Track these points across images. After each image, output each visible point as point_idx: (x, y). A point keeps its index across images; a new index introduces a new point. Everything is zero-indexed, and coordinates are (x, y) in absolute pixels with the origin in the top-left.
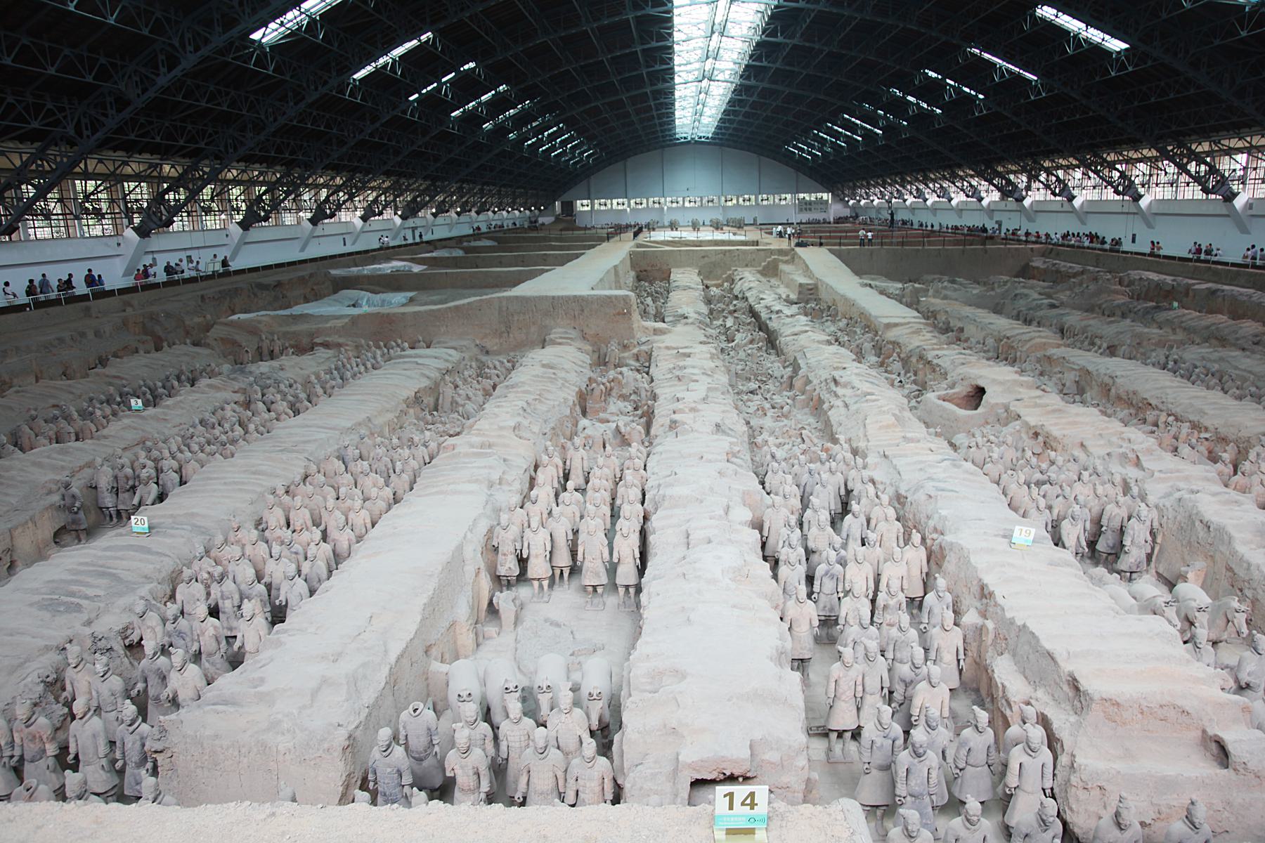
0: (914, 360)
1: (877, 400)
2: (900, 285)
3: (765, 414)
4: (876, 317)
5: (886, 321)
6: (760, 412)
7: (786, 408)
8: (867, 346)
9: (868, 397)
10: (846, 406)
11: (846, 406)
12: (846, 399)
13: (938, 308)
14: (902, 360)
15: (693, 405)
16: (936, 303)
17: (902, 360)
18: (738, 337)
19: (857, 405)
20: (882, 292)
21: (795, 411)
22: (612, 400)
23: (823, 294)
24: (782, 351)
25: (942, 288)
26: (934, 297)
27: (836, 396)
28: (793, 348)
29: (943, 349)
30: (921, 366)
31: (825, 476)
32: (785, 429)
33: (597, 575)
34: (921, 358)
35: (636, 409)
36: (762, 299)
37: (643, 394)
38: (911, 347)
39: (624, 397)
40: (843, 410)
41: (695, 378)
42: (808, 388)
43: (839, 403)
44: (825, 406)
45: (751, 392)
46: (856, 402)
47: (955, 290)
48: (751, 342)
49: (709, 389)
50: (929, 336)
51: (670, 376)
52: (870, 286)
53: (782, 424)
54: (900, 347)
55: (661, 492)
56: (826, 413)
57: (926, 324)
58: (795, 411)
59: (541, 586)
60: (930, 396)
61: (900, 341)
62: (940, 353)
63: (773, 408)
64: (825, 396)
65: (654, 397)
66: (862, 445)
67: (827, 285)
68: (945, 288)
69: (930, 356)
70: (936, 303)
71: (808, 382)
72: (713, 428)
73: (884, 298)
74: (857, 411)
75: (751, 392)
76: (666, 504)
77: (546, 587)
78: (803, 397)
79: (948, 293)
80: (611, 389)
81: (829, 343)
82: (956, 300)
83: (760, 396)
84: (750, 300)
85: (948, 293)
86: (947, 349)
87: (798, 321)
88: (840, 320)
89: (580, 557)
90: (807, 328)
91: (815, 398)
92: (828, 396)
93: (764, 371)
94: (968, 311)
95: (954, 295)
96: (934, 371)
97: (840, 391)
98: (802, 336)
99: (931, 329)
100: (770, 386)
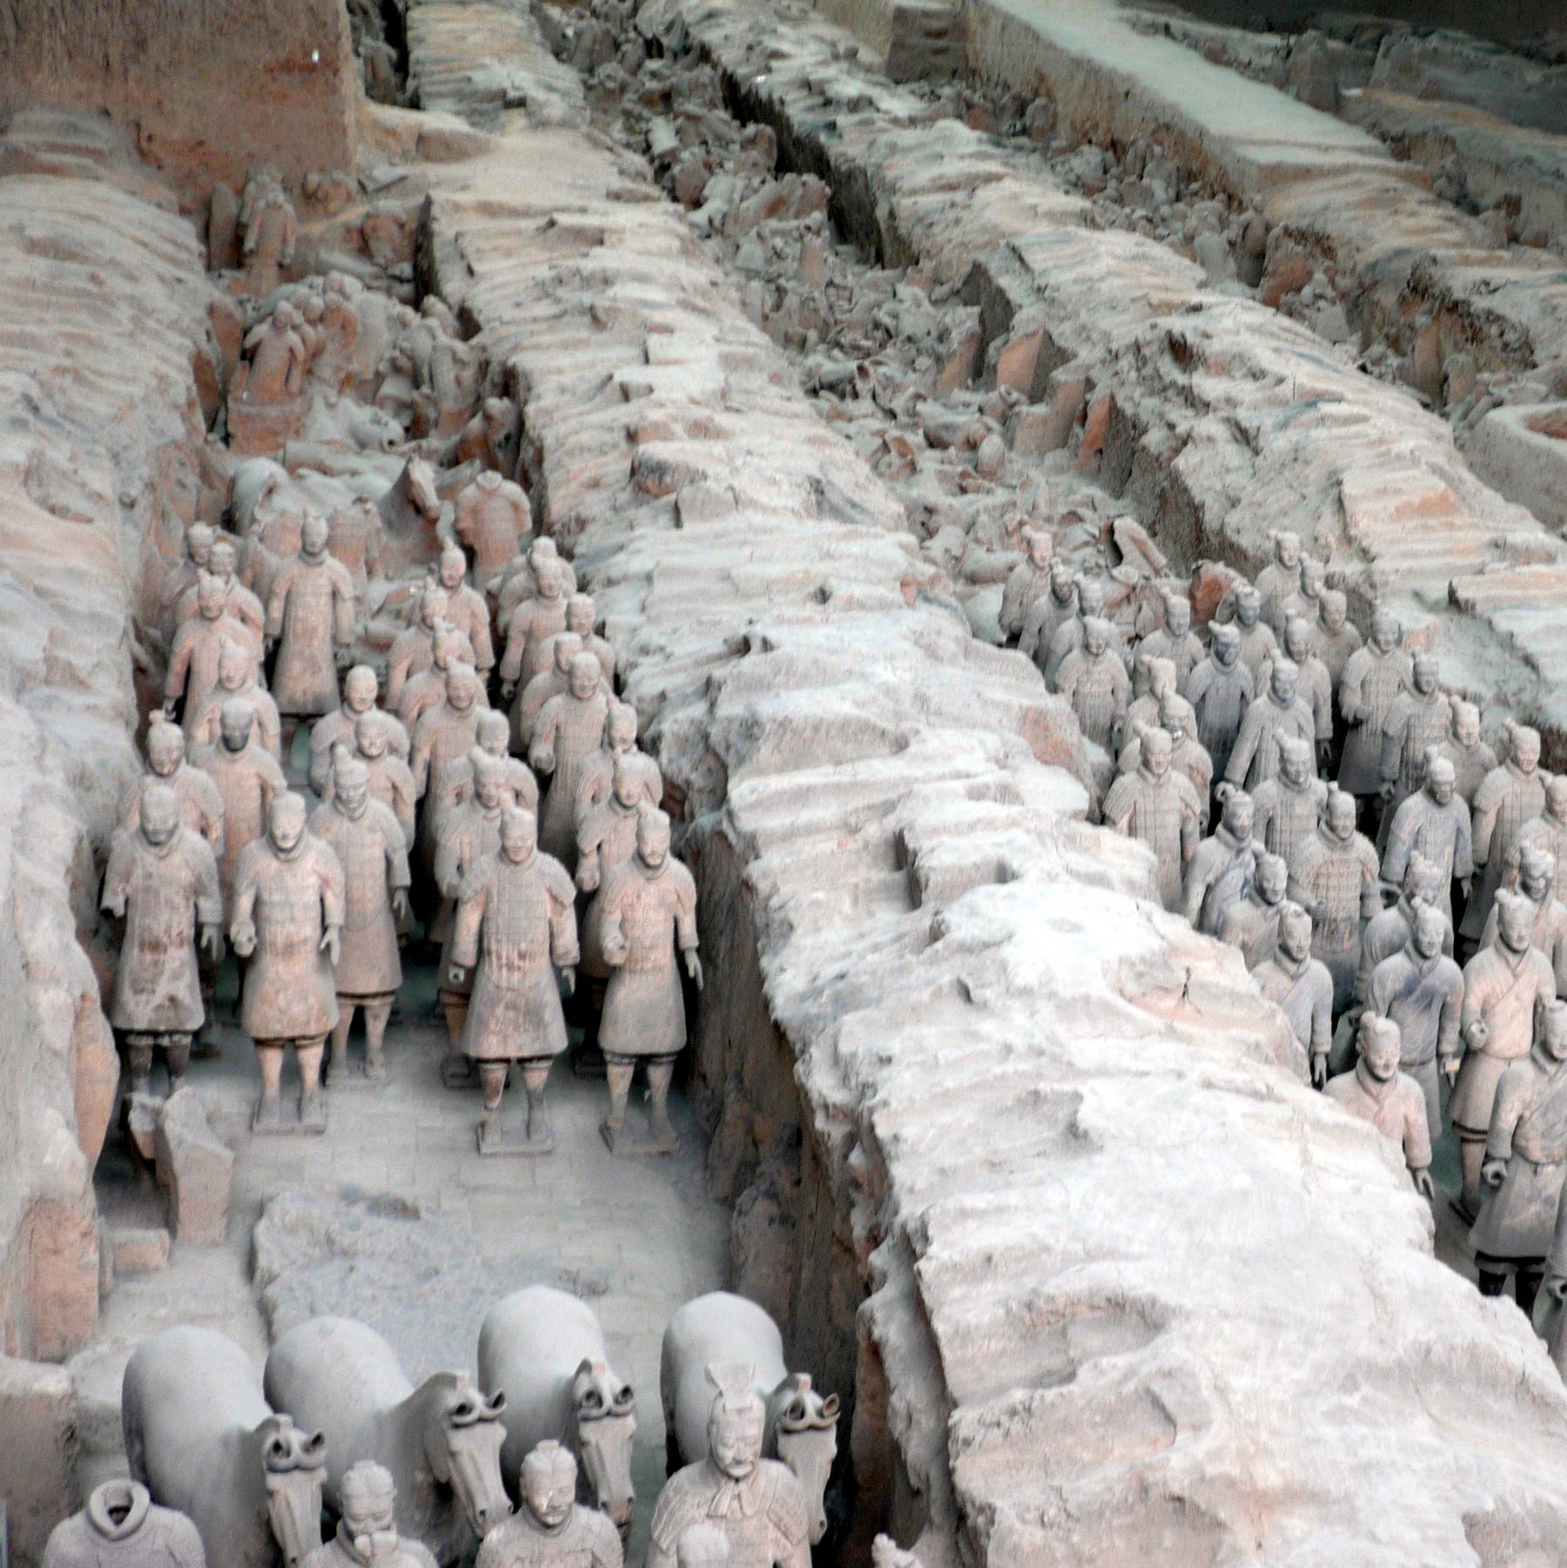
0: (1387, 298)
1: (1365, 419)
2: (1272, 40)
3: (913, 468)
4: (1226, 142)
5: (1266, 156)
6: (894, 457)
7: (991, 446)
8: (1212, 241)
9: (1327, 408)
10: (1245, 437)
11: (1245, 437)
12: (1244, 415)
13: (1414, 127)
14: (1343, 296)
15: (701, 413)
16: (1409, 109)
17: (1343, 296)
18: (720, 192)
19: (1294, 434)
20: (1217, 56)
21: (1017, 462)
22: (321, 393)
23: (988, 49)
24: (902, 243)
25: (1424, 56)
26: (1397, 87)
27: (1192, 400)
28: (956, 234)
29: (1499, 262)
30: (1421, 320)
31: (1286, 666)
32: (1012, 518)
33: (533, 1015)
34: (1418, 289)
35: (416, 429)
36: (776, 55)
37: (447, 375)
38: (1373, 253)
39: (366, 389)
40: (1232, 454)
41: (658, 317)
42: (1060, 375)
43: (1209, 426)
44: (1154, 439)
45: (831, 387)
46: (1284, 425)
47: (1468, 67)
48: (775, 208)
49: (729, 362)
50: (1431, 215)
51: (544, 309)
52: (1167, 30)
53: (983, 501)
54: (1328, 252)
55: (731, 707)
56: (1159, 463)
57: (1408, 177)
58: (1017, 462)
59: (292, 1073)
60: (1509, 419)
61: (1331, 229)
62: (1497, 274)
63: (934, 442)
64: (1139, 403)
65: (509, 383)
66: (1351, 569)
67: (1008, 21)
68: (1433, 56)
69: (1460, 280)
70: (1409, 109)
71: (1052, 354)
72: (798, 498)
73: (1229, 77)
74: (1297, 455)
75: (831, 387)
76: (765, 752)
77: (311, 1074)
78: (1040, 409)
79: (1447, 76)
80: (316, 353)
81: (1088, 221)
82: (1471, 101)
83: (865, 405)
84: (729, 57)
85: (1447, 76)
86: (1511, 263)
87: (947, 139)
88: (1062, 151)
89: (464, 947)
90: (994, 167)
91: (1097, 412)
92: (1151, 403)
93: (857, 315)
94: (1524, 142)
95: (1465, 84)
96: (1476, 337)
97: (1207, 385)
98: (984, 194)
99: (1421, 194)
100: (890, 366)
